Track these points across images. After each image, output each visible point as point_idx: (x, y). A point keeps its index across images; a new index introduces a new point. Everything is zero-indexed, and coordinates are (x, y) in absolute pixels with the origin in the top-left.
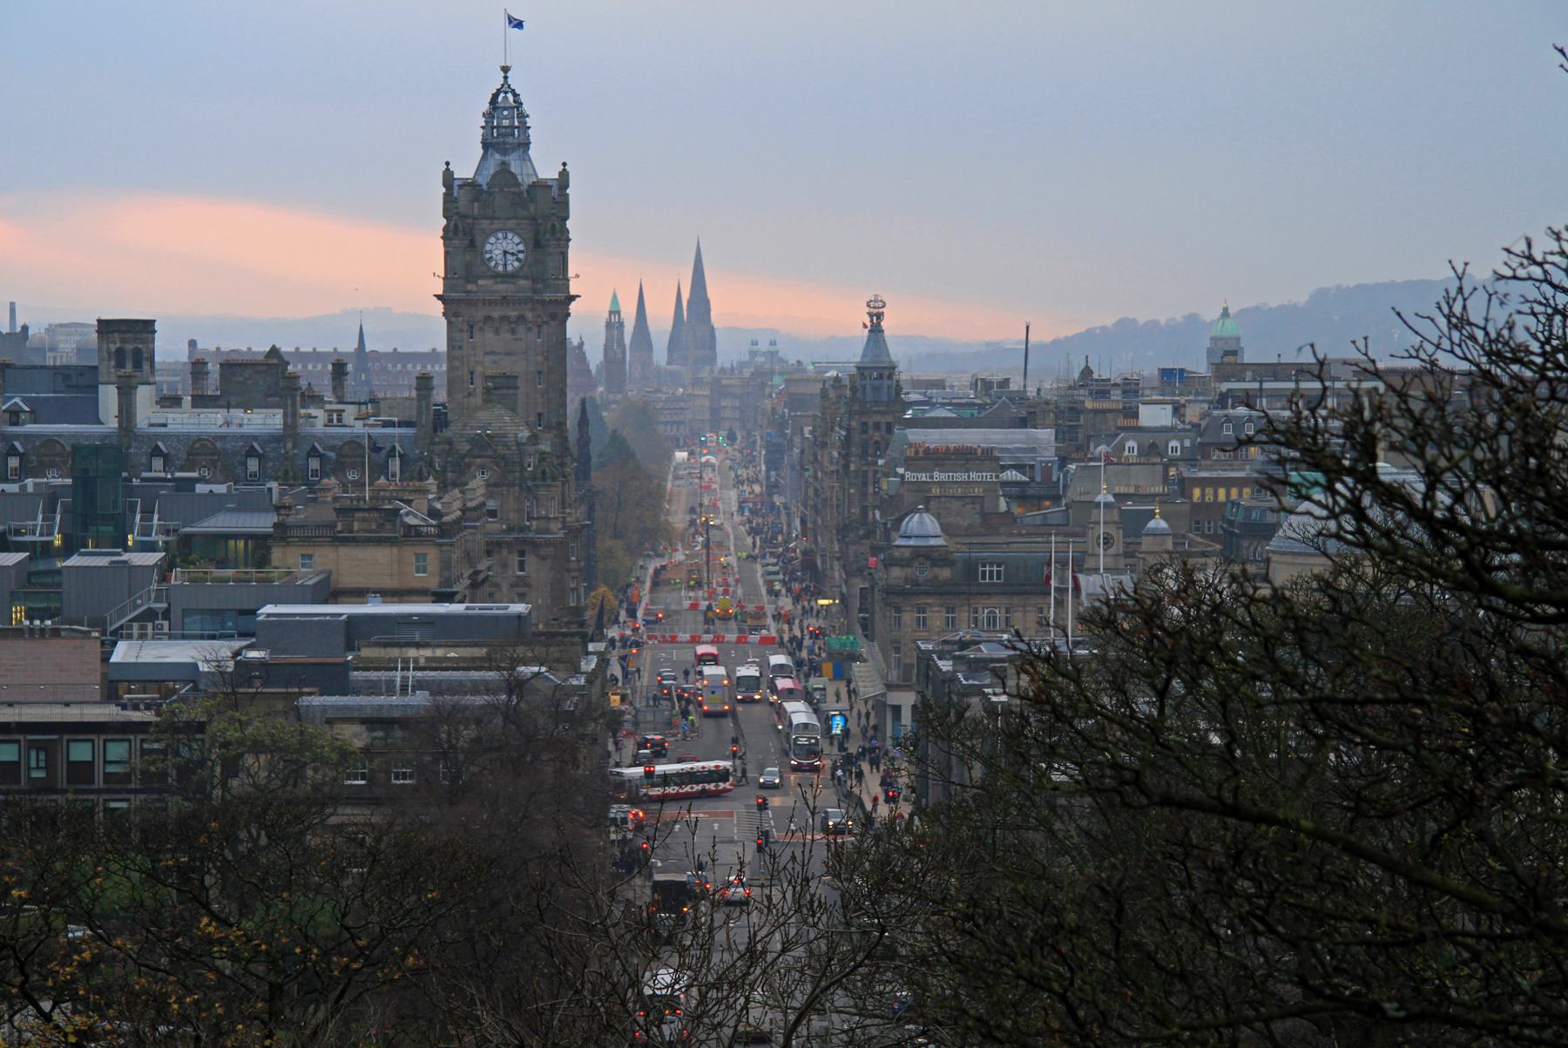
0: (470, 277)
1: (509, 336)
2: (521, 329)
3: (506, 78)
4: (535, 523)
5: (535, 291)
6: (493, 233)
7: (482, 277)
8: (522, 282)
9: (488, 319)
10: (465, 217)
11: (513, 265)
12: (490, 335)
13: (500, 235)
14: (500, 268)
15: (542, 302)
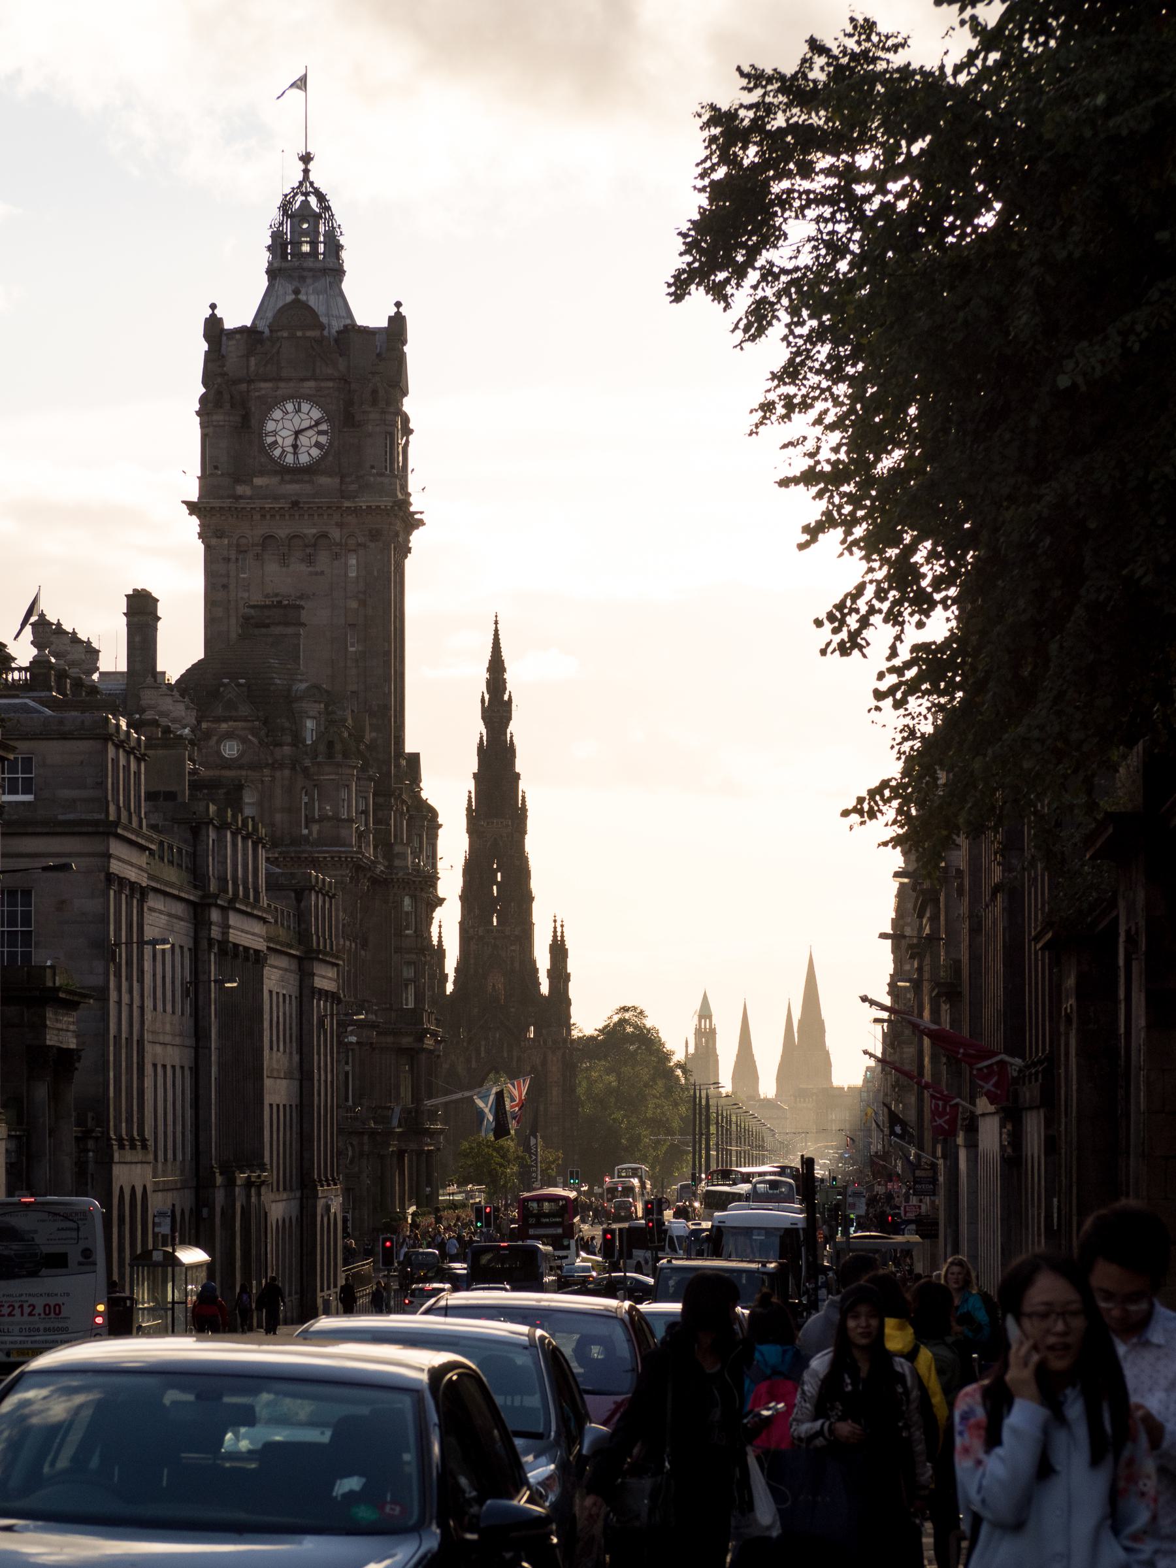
0: (239, 476)
1: (303, 568)
2: (323, 558)
3: (306, 172)
4: (315, 828)
5: (344, 495)
6: (279, 401)
7: (262, 473)
8: (324, 480)
9: (268, 538)
10: (236, 382)
11: (308, 454)
12: (272, 568)
13: (290, 407)
14: (290, 459)
15: (356, 511)
